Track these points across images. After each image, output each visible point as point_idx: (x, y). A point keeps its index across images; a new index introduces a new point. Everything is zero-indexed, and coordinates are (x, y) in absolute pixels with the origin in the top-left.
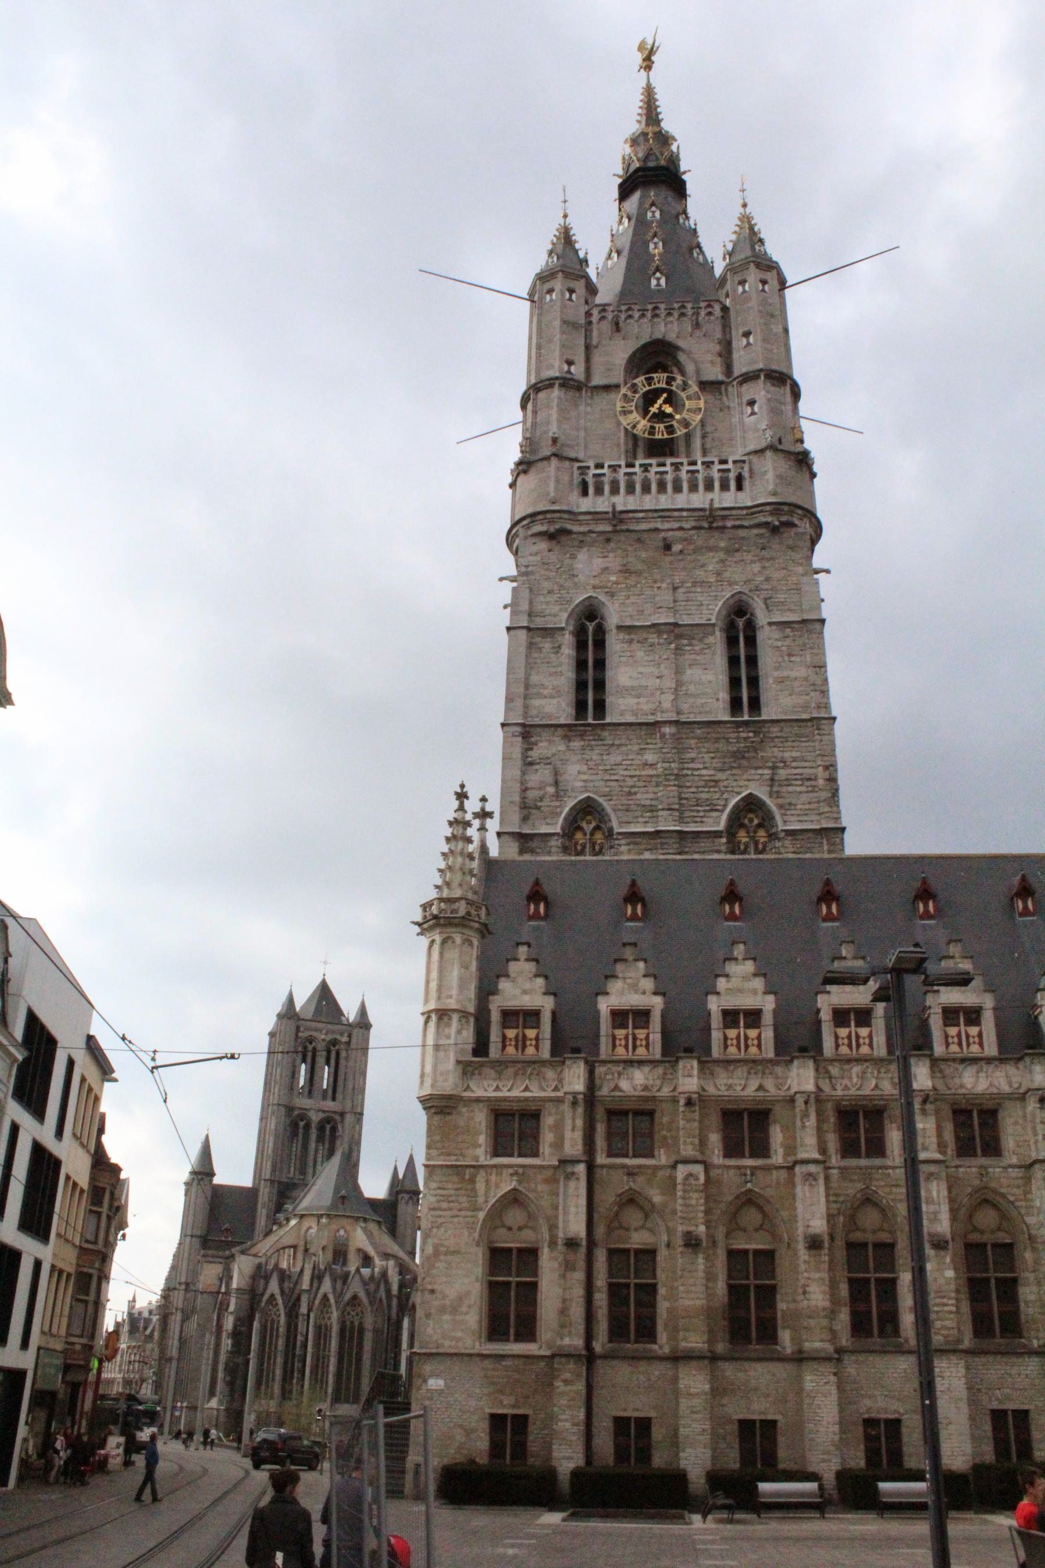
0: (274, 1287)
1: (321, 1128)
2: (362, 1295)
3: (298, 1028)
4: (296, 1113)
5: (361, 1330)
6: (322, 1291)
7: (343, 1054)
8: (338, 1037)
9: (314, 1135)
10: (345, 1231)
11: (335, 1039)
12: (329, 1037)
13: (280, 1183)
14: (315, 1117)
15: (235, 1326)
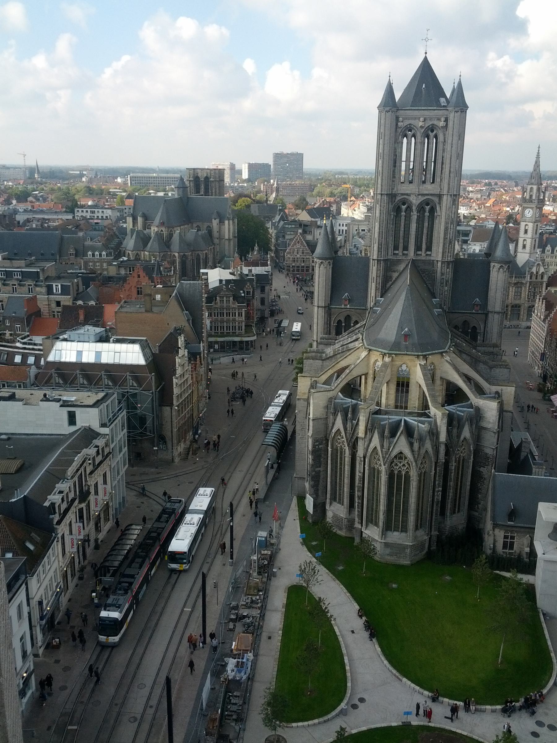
0: (339, 424)
1: (421, 209)
2: (407, 452)
3: (397, 118)
4: (398, 198)
5: (407, 477)
6: (372, 446)
7: (441, 138)
8: (436, 122)
9: (414, 216)
10: (407, 366)
11: (433, 124)
12: (429, 123)
13: (385, 261)
14: (415, 201)
15: (314, 446)
